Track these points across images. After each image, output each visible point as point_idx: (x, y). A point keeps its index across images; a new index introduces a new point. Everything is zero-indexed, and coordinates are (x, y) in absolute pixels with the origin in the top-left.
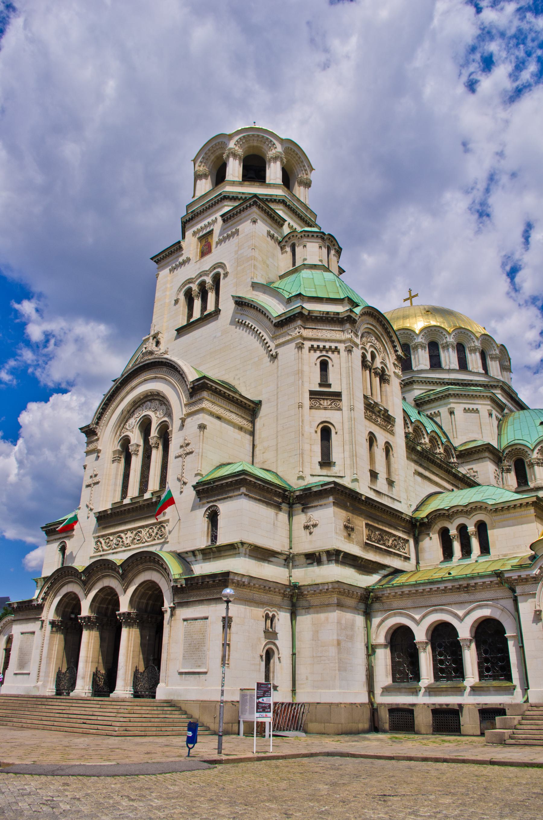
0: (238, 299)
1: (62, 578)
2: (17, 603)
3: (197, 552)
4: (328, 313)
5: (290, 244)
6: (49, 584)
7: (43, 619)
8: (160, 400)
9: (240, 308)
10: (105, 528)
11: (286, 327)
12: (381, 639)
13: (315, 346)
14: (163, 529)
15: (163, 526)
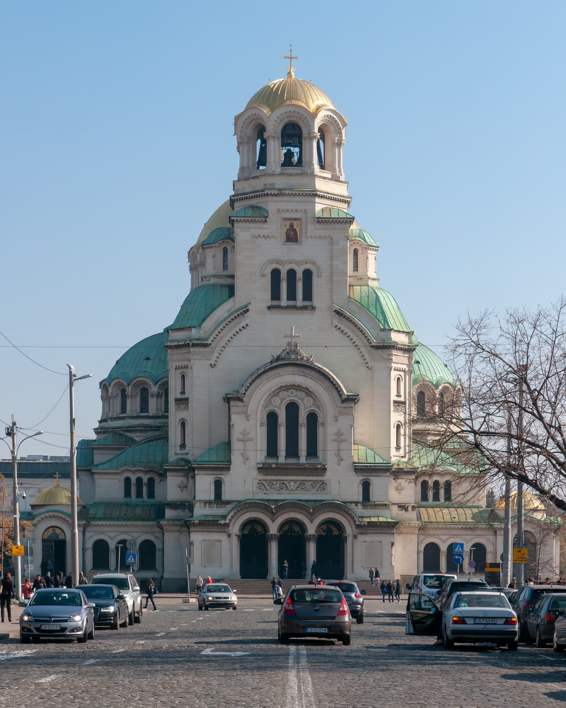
0: (338, 310)
1: (247, 508)
2: (200, 521)
3: (359, 504)
4: (405, 345)
5: (353, 249)
6: (235, 511)
7: (230, 533)
8: (306, 393)
9: (337, 315)
10: (264, 475)
11: (380, 350)
12: (422, 548)
13: (396, 368)
14: (324, 485)
15: (325, 483)
